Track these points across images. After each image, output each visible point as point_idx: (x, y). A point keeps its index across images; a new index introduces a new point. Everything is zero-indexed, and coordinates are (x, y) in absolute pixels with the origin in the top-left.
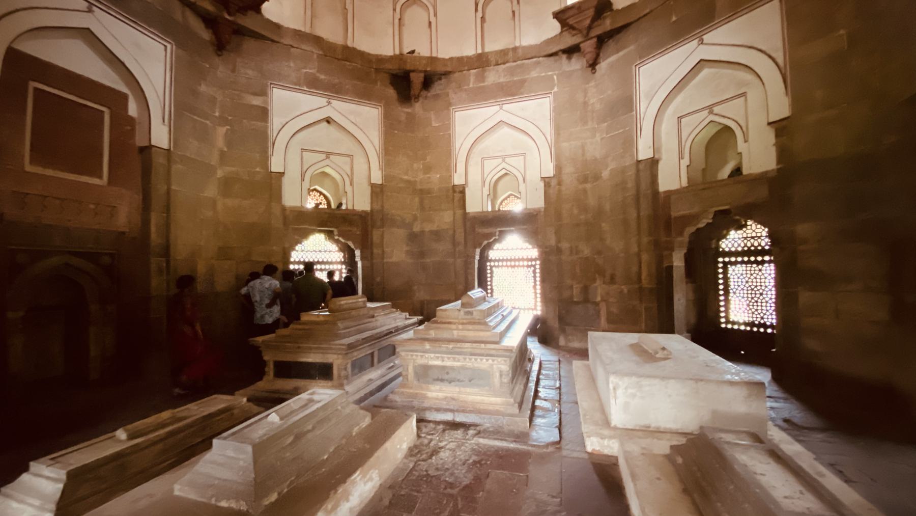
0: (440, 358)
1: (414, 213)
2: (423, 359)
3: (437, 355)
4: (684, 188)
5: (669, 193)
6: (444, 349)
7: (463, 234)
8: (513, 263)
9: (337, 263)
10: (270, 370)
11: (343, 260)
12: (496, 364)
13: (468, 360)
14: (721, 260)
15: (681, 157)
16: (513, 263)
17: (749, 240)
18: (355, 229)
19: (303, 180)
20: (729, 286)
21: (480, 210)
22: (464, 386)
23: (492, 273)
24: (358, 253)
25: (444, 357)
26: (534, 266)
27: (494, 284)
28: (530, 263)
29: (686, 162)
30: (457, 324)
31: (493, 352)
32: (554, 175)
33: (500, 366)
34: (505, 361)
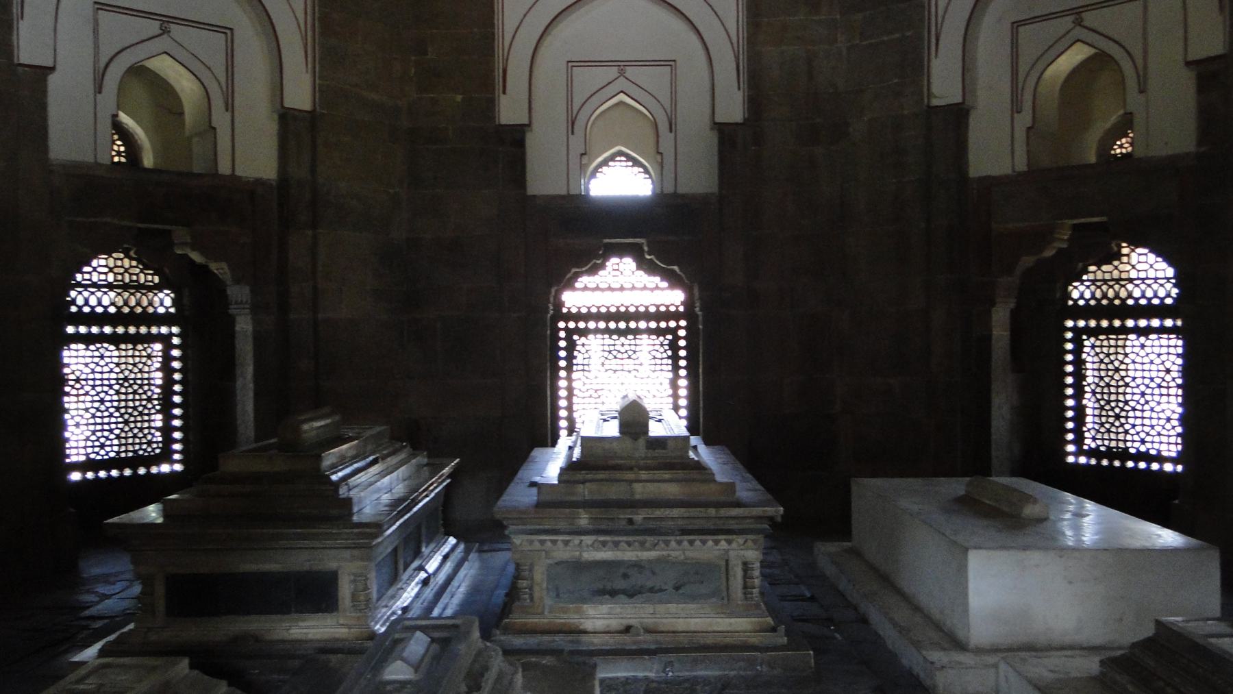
0: (610, 544)
2: (568, 548)
3: (602, 538)
4: (1020, 174)
5: (990, 182)
6: (623, 524)
8: (622, 325)
13: (673, 544)
14: (1070, 323)
15: (1016, 108)
16: (622, 325)
17: (1123, 286)
19: (99, 89)
20: (1084, 377)
21: (563, 192)
22: (660, 602)
23: (571, 347)
24: (239, 293)
25: (620, 542)
26: (673, 331)
28: (663, 325)
29: (1024, 119)
30: (636, 469)
31: (733, 525)
32: (745, 119)
33: (742, 552)
34: (754, 541)
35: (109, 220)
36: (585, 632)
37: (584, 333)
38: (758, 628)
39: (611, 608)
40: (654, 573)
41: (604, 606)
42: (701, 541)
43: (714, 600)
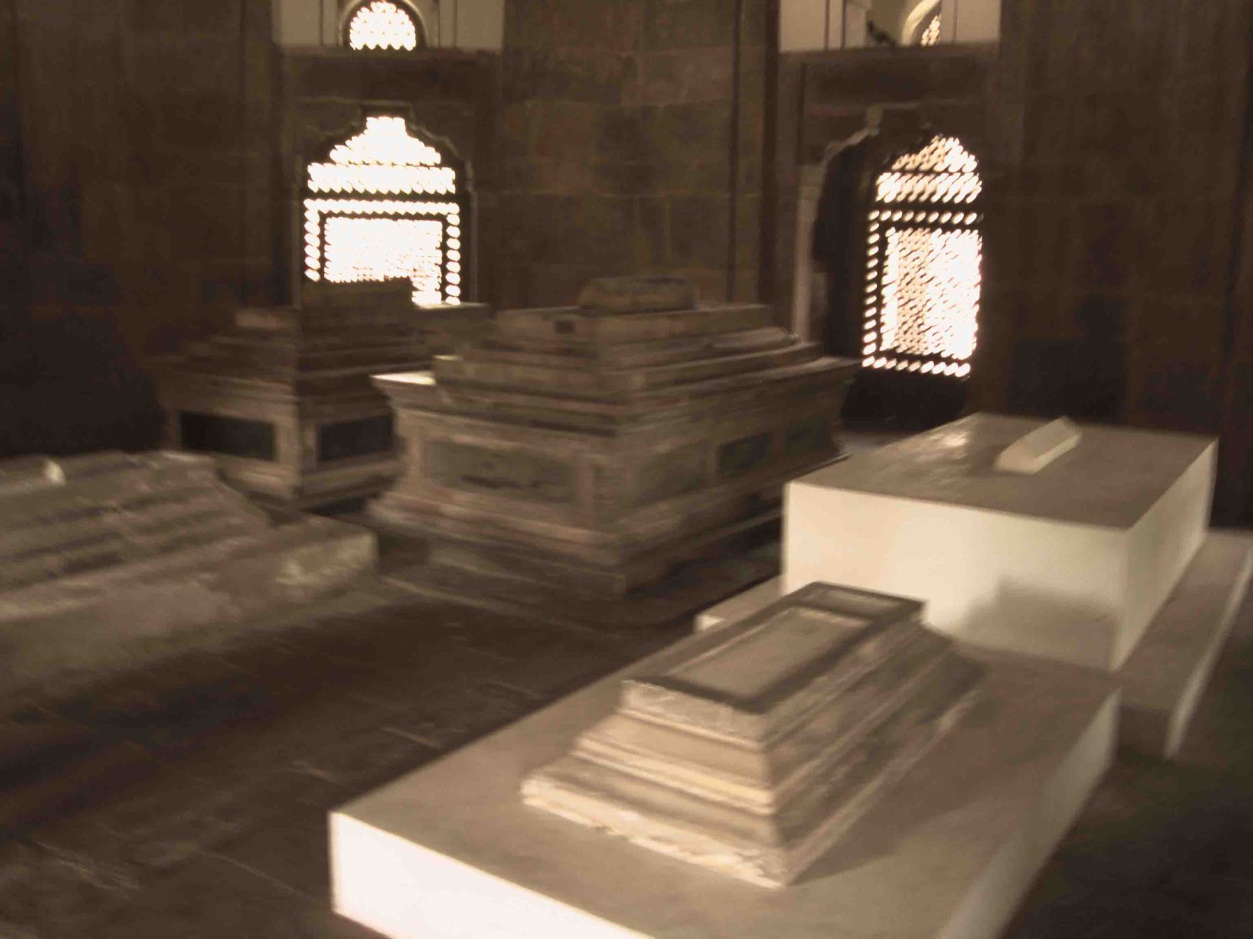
1: (624, 55)
3: (468, 421)
9: (436, 198)
10: (173, 428)
11: (453, 189)
21: (819, 45)
23: (883, 243)
27: (885, 280)
36: (441, 515)
37: (901, 226)
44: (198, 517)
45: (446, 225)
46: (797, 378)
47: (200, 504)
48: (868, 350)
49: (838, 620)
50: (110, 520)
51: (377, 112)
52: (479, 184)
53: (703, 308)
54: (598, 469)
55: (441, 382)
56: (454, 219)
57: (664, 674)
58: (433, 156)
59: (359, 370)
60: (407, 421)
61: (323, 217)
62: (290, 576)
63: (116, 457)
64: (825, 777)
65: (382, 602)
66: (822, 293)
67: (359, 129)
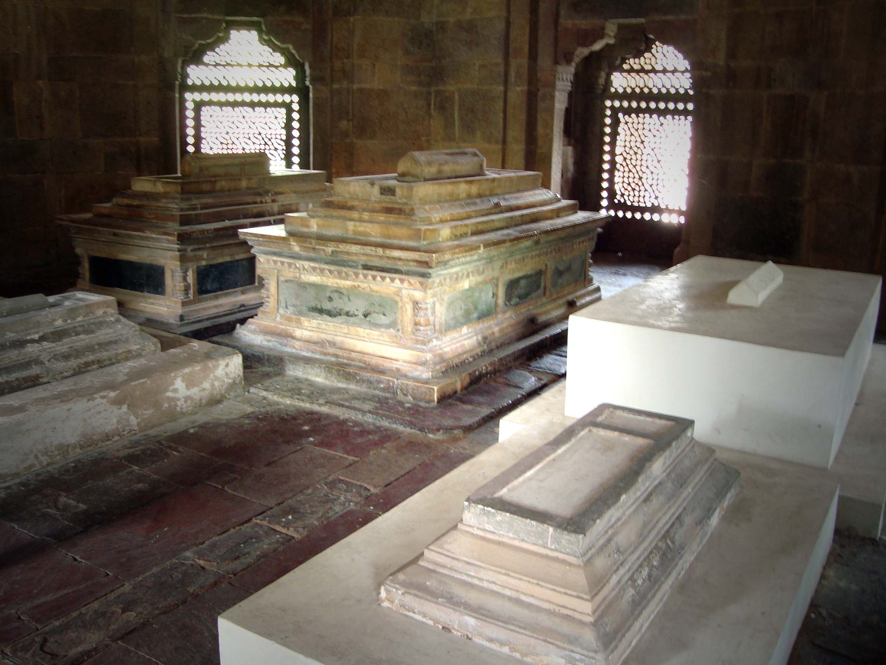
3: (312, 264)
7: (527, 30)
8: (662, 105)
9: (283, 90)
10: (85, 269)
11: (294, 84)
12: (406, 289)
13: (361, 276)
18: (299, 19)
22: (354, 324)
23: (616, 123)
25: (324, 269)
27: (618, 150)
31: (400, 265)
35: (205, 15)
36: (293, 338)
37: (628, 112)
38: (414, 361)
39: (319, 324)
40: (349, 300)
41: (314, 321)
42: (390, 278)
43: (392, 330)
44: (103, 345)
45: (290, 111)
46: (563, 228)
47: (103, 334)
48: (604, 203)
49: (627, 438)
50: (31, 349)
51: (240, 25)
52: (314, 80)
53: (491, 174)
54: (416, 304)
55: (291, 234)
56: (296, 107)
57: (496, 495)
58: (279, 59)
59: (227, 223)
60: (264, 264)
61: (198, 106)
62: (175, 391)
63: (38, 298)
64: (632, 578)
65: (249, 410)
66: (571, 161)
67: (225, 39)
